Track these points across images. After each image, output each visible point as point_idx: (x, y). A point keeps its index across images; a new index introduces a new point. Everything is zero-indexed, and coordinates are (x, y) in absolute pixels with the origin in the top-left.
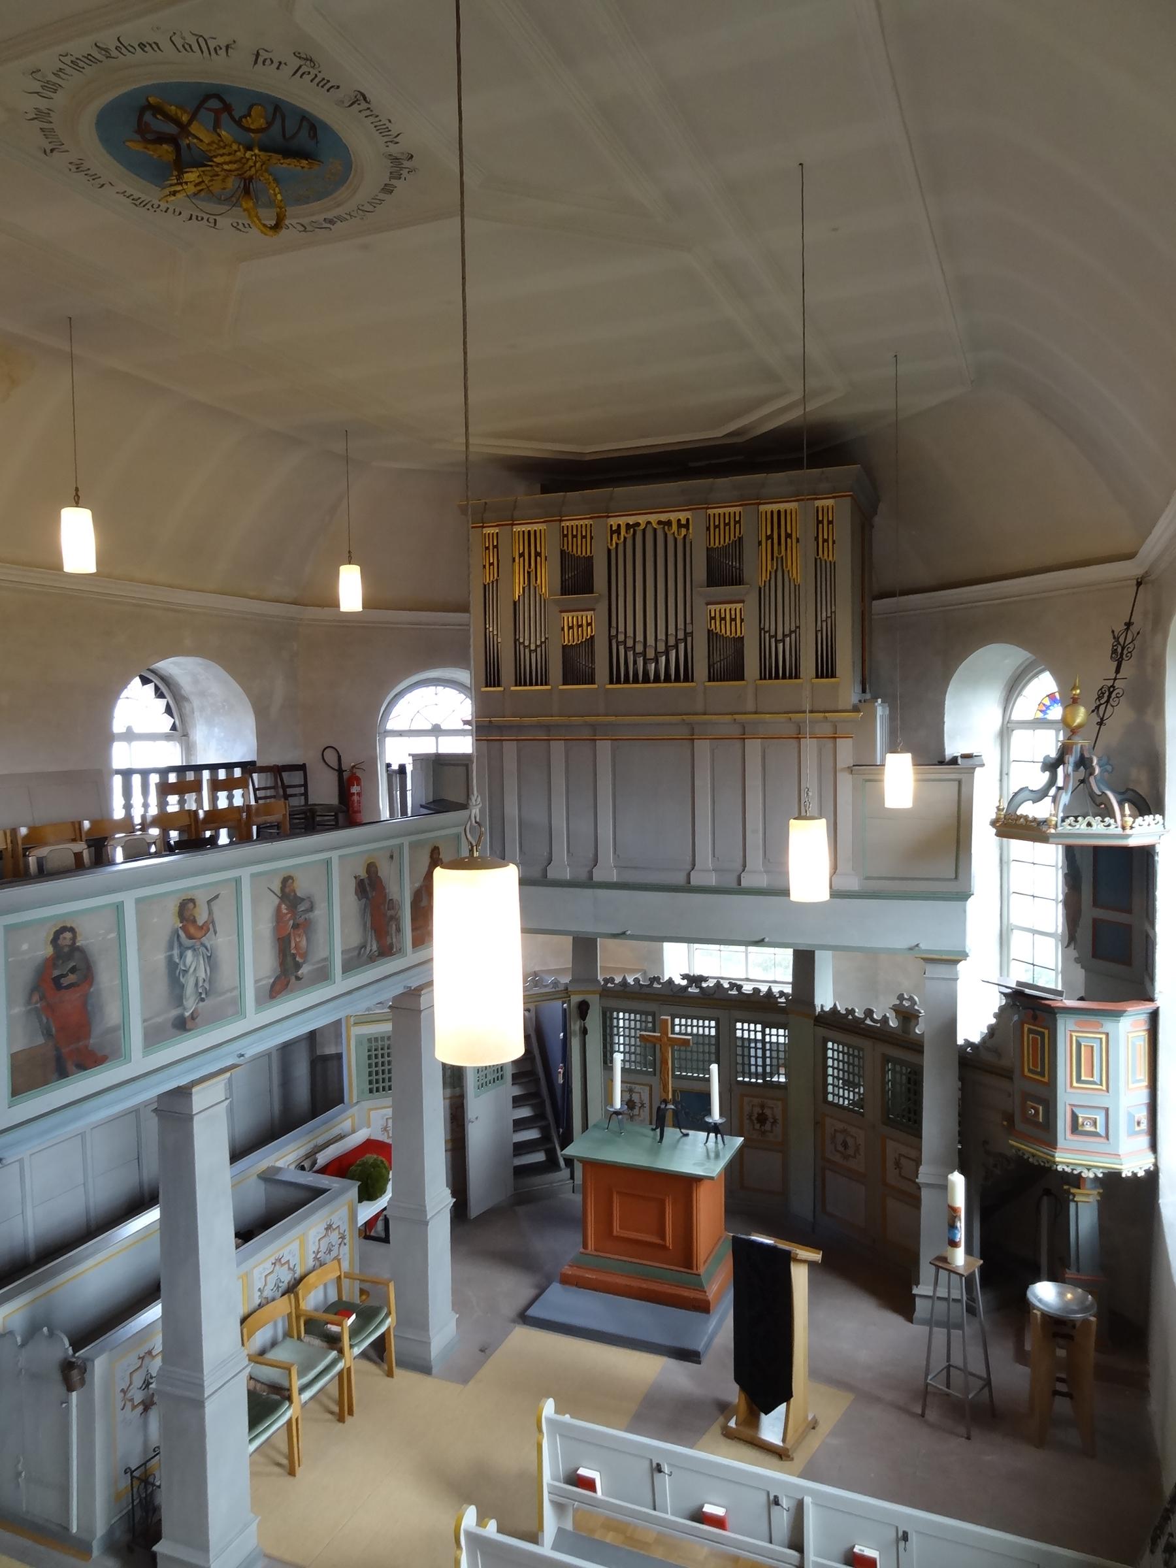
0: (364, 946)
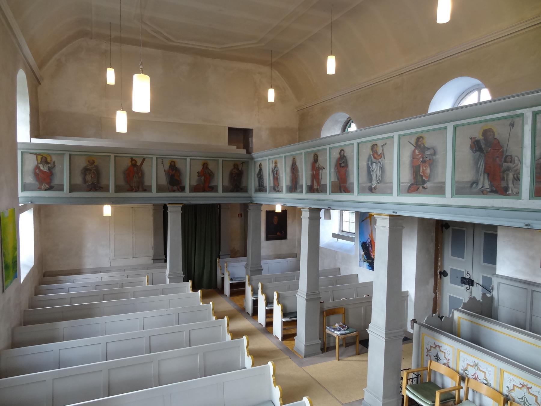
0: (476, 182)
